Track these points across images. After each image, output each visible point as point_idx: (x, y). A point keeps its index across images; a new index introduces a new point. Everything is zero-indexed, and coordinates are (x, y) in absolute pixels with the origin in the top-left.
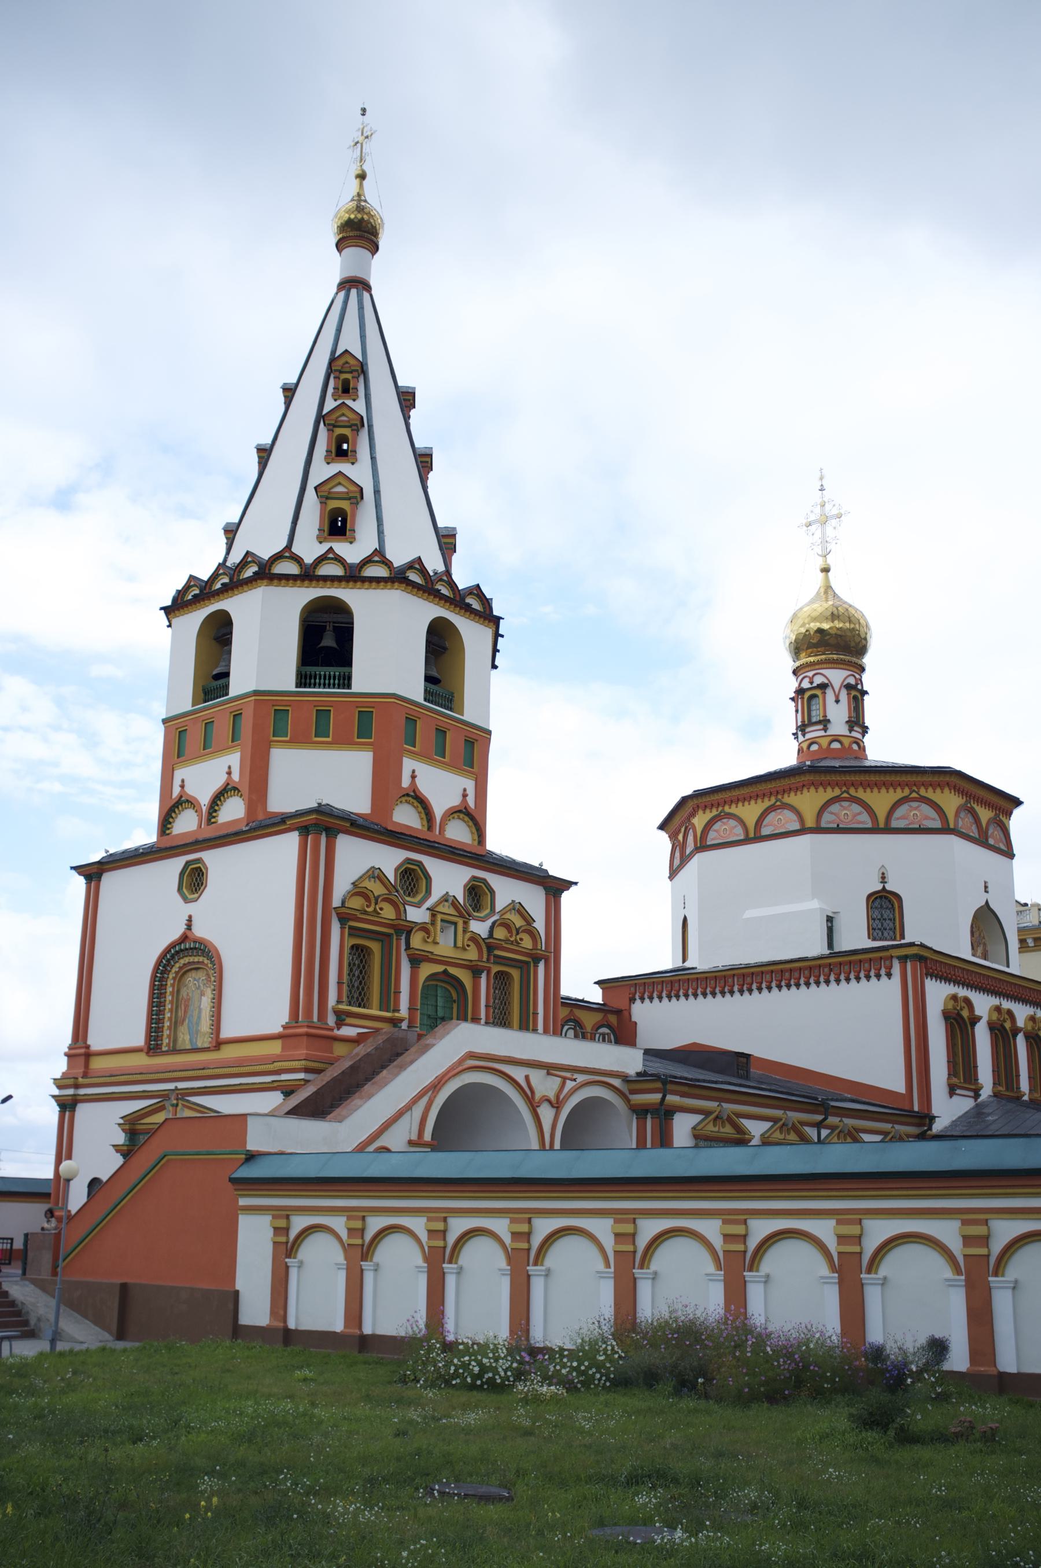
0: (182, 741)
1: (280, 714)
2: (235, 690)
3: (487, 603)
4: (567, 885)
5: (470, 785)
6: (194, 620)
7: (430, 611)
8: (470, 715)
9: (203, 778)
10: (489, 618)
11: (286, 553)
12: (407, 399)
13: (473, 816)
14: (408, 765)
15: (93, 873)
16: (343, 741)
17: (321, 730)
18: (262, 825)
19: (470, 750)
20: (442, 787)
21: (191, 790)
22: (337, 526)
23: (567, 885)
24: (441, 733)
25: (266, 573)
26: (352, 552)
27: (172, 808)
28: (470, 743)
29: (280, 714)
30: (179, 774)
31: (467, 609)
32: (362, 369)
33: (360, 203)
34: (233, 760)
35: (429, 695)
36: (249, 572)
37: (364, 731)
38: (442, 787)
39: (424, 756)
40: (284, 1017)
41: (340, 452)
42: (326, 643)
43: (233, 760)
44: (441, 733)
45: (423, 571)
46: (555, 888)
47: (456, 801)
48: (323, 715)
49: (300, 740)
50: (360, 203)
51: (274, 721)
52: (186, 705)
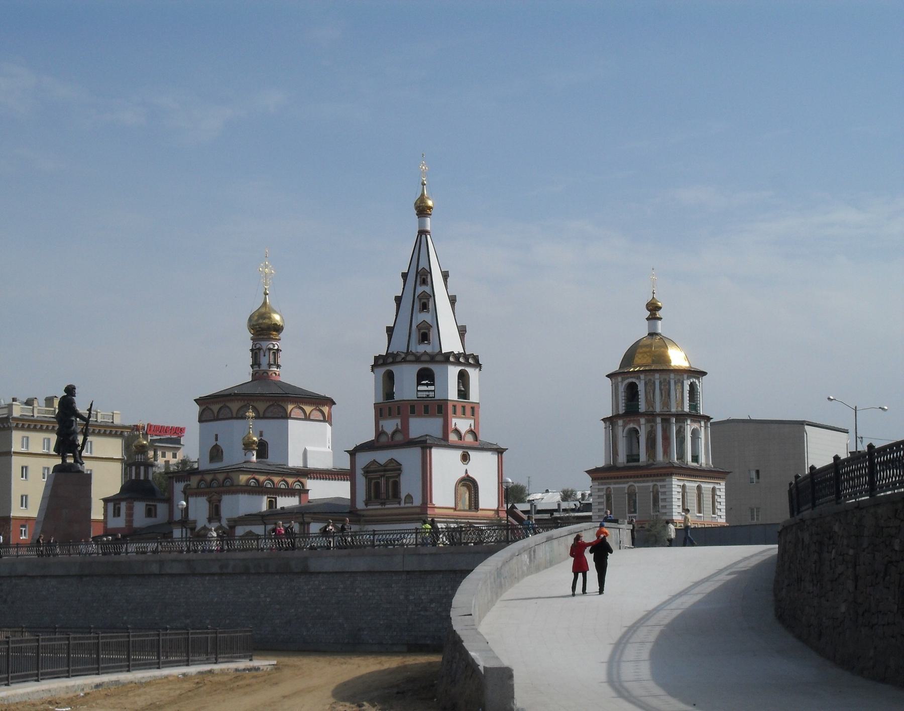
0: (381, 412)
1: (413, 407)
2: (397, 397)
3: (476, 358)
5: (472, 422)
6: (382, 371)
7: (459, 368)
9: (390, 425)
10: (477, 365)
14: (454, 421)
15: (353, 453)
16: (433, 415)
18: (411, 443)
19: (473, 410)
20: (462, 424)
21: (385, 429)
24: (464, 407)
27: (379, 433)
28: (473, 408)
29: (413, 407)
30: (381, 423)
31: (470, 365)
34: (398, 421)
36: (399, 359)
40: (421, 502)
41: (424, 307)
43: (398, 421)
44: (464, 407)
45: (455, 355)
46: (500, 451)
47: (468, 428)
49: (420, 416)
52: (381, 400)
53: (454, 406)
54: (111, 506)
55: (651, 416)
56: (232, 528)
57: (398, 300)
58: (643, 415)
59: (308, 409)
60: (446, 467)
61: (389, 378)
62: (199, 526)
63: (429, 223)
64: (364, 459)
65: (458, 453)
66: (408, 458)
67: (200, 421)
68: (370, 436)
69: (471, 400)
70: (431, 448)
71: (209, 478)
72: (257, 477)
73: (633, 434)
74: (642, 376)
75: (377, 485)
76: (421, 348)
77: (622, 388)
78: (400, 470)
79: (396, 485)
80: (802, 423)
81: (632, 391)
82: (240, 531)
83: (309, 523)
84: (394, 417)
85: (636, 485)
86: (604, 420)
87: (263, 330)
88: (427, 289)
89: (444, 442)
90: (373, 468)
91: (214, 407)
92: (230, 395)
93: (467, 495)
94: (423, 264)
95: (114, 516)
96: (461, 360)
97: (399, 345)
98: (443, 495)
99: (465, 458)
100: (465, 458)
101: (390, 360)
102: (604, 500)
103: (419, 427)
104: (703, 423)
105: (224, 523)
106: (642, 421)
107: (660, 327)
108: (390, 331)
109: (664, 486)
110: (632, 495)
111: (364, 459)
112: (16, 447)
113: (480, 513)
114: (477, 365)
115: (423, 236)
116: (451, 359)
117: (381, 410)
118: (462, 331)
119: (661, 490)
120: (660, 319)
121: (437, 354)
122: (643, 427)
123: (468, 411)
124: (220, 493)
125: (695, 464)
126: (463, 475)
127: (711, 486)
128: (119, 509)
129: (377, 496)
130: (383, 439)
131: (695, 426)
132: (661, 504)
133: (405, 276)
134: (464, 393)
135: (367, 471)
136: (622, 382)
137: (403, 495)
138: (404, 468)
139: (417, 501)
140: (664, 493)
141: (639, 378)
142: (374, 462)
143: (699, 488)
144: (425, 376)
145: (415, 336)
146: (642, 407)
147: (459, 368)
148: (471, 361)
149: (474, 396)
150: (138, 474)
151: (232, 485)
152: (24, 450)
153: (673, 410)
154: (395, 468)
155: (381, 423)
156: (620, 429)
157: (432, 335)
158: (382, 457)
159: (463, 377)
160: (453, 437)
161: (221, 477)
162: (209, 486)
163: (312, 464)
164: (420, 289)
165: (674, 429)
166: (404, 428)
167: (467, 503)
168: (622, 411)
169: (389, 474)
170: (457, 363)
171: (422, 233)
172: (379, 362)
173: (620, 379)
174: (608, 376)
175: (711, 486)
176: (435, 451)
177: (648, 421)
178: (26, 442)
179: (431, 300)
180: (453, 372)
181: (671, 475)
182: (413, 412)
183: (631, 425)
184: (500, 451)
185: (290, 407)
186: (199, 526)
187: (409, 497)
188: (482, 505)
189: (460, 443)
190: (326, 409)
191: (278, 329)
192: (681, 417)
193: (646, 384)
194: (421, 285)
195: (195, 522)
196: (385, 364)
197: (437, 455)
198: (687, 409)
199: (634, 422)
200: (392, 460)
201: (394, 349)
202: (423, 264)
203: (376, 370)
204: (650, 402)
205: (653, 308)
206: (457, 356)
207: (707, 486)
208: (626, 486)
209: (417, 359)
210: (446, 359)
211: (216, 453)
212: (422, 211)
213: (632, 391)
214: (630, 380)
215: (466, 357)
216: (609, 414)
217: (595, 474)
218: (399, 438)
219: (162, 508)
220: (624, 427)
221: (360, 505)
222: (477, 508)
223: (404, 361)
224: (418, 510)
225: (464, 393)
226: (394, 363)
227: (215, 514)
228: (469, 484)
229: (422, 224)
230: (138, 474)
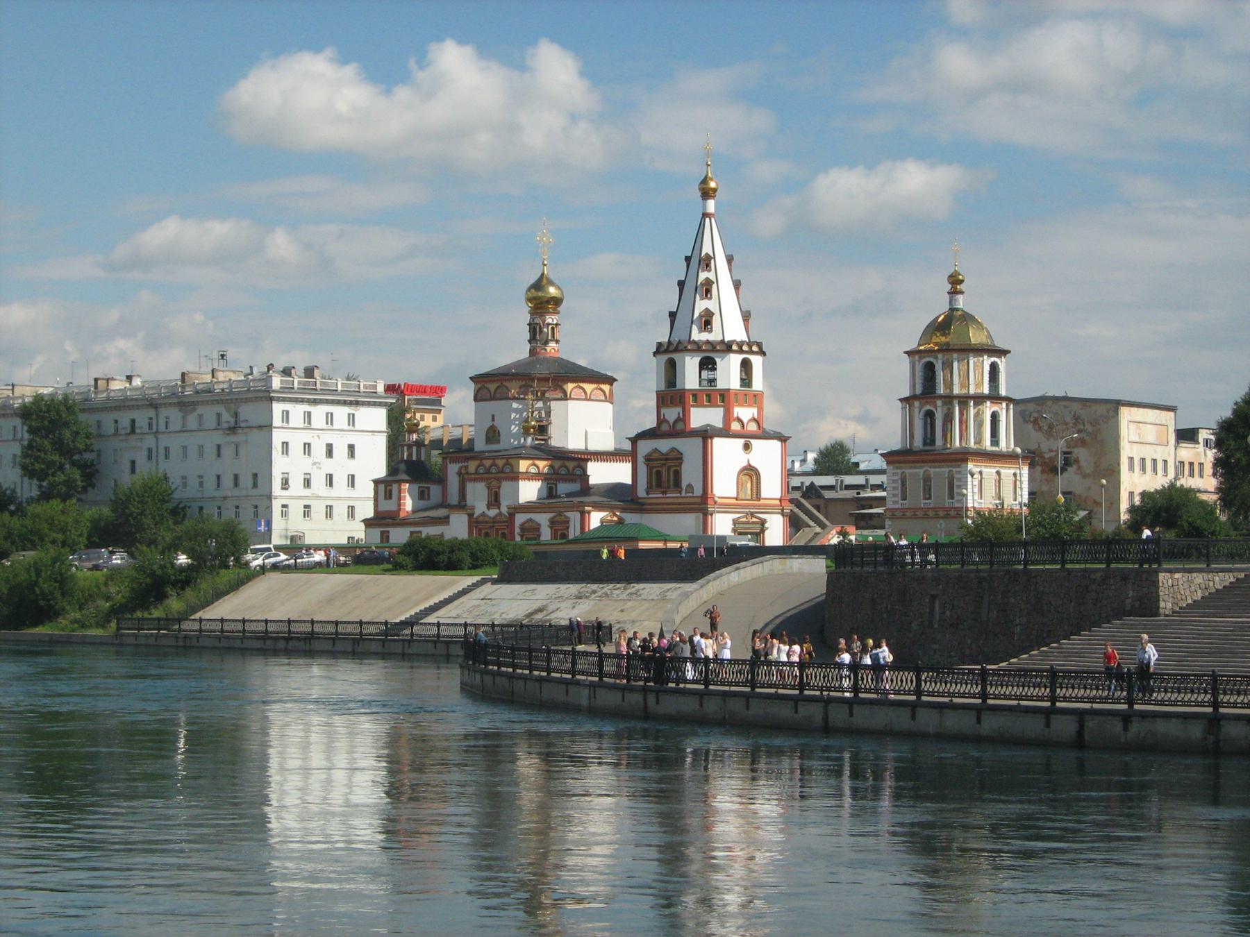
2: (678, 387)
3: (759, 345)
6: (665, 357)
7: (740, 357)
9: (671, 414)
15: (634, 441)
19: (755, 399)
20: (745, 413)
27: (661, 420)
31: (752, 352)
34: (680, 410)
39: (741, 405)
43: (680, 410)
52: (663, 387)
54: (382, 487)
55: (949, 399)
56: (512, 515)
58: (941, 397)
59: (589, 387)
60: (727, 458)
62: (477, 512)
63: (711, 206)
64: (645, 447)
65: (742, 441)
66: (689, 447)
67: (476, 399)
68: (650, 422)
70: (712, 438)
71: (488, 463)
72: (537, 462)
73: (930, 415)
74: (940, 356)
75: (659, 474)
76: (704, 336)
77: (919, 368)
78: (681, 459)
79: (678, 475)
80: (1119, 403)
81: (930, 370)
82: (520, 518)
83: (589, 513)
85: (932, 470)
86: (901, 400)
87: (541, 303)
88: (711, 275)
89: (725, 433)
90: (655, 456)
91: (491, 386)
92: (507, 375)
93: (749, 485)
95: (386, 498)
96: (745, 348)
98: (724, 484)
99: (747, 447)
100: (747, 447)
102: (899, 485)
103: (700, 417)
104: (1004, 404)
105: (504, 510)
106: (939, 403)
107: (961, 302)
109: (959, 472)
110: (927, 480)
111: (645, 447)
112: (277, 421)
113: (762, 502)
114: (762, 352)
116: (735, 347)
118: (746, 317)
119: (956, 476)
120: (962, 292)
122: (939, 409)
124: (499, 480)
125: (995, 449)
126: (745, 464)
127: (1012, 471)
128: (391, 491)
129: (659, 485)
130: (665, 427)
131: (995, 408)
132: (956, 490)
134: (746, 380)
135: (648, 459)
136: (920, 359)
137: (684, 485)
138: (686, 459)
139: (698, 491)
140: (959, 480)
141: (936, 358)
142: (656, 450)
143: (998, 473)
144: (708, 364)
146: (941, 390)
147: (740, 357)
148: (755, 348)
149: (758, 383)
150: (410, 455)
151: (512, 471)
152: (285, 425)
153: (972, 392)
154: (676, 458)
155: (663, 411)
156: (917, 411)
157: (716, 321)
158: (664, 445)
159: (746, 366)
160: (735, 426)
161: (500, 463)
162: (488, 471)
163: (592, 447)
165: (972, 411)
166: (684, 418)
167: (749, 492)
168: (919, 391)
169: (670, 463)
170: (741, 351)
172: (660, 350)
173: (917, 357)
174: (908, 353)
175: (1012, 471)
176: (717, 441)
177: (944, 404)
178: (286, 415)
179: (714, 286)
180: (735, 360)
181: (966, 461)
183: (928, 407)
184: (783, 439)
185: (570, 387)
186: (477, 512)
187: (690, 486)
188: (763, 496)
190: (606, 388)
191: (557, 302)
192: (979, 399)
193: (943, 363)
195: (473, 508)
196: (667, 351)
197: (718, 444)
198: (986, 391)
199: (930, 403)
200: (673, 449)
201: (675, 339)
202: (707, 249)
204: (950, 385)
205: (955, 281)
206: (740, 344)
207: (1007, 472)
208: (921, 471)
210: (727, 347)
211: (493, 435)
213: (930, 370)
214: (928, 359)
216: (907, 394)
217: (890, 457)
218: (680, 426)
219: (435, 490)
220: (920, 408)
221: (641, 492)
222: (759, 498)
223: (685, 350)
224: (699, 500)
225: (746, 380)
226: (676, 350)
227: (494, 501)
228: (750, 473)
229: (704, 207)
230: (410, 455)
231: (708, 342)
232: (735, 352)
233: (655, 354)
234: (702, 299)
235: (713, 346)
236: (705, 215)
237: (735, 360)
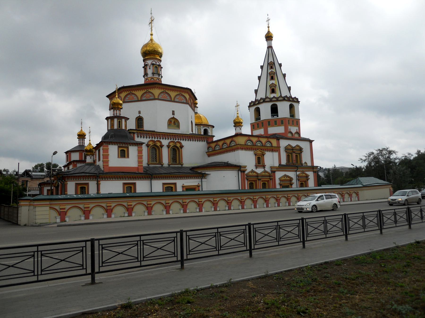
1: (269, 122)
2: (262, 119)
3: (297, 99)
4: (313, 141)
5: (297, 128)
6: (253, 108)
7: (290, 103)
8: (296, 117)
11: (267, 98)
12: (280, 65)
13: (298, 133)
14: (289, 127)
16: (279, 125)
17: (276, 123)
19: (297, 123)
20: (293, 129)
22: (273, 91)
23: (313, 141)
25: (264, 101)
26: (277, 95)
28: (297, 122)
29: (269, 122)
31: (294, 101)
32: (274, 63)
33: (269, 32)
35: (291, 116)
36: (262, 101)
37: (282, 123)
38: (293, 129)
39: (291, 126)
42: (274, 110)
46: (311, 142)
47: (295, 131)
48: (276, 122)
49: (273, 126)
50: (269, 32)
51: (269, 123)
52: (254, 121)
53: (289, 121)
57: (259, 78)
61: (258, 111)
69: (296, 118)
84: (260, 128)
94: (271, 60)
97: (262, 95)
101: (257, 102)
108: (256, 91)
115: (270, 49)
117: (253, 125)
121: (279, 97)
123: (295, 122)
133: (262, 67)
145: (269, 91)
147: (288, 103)
164: (270, 71)
170: (289, 100)
171: (270, 47)
180: (288, 104)
182: (269, 125)
189: (292, 137)
194: (270, 69)
196: (254, 105)
201: (259, 98)
203: (250, 108)
209: (271, 100)
212: (269, 37)
215: (293, 99)
225: (292, 115)
226: (259, 103)
231: (274, 97)
232: (286, 100)
233: (249, 107)
234: (270, 80)
235: (277, 100)
236: (270, 47)
237: (288, 104)
